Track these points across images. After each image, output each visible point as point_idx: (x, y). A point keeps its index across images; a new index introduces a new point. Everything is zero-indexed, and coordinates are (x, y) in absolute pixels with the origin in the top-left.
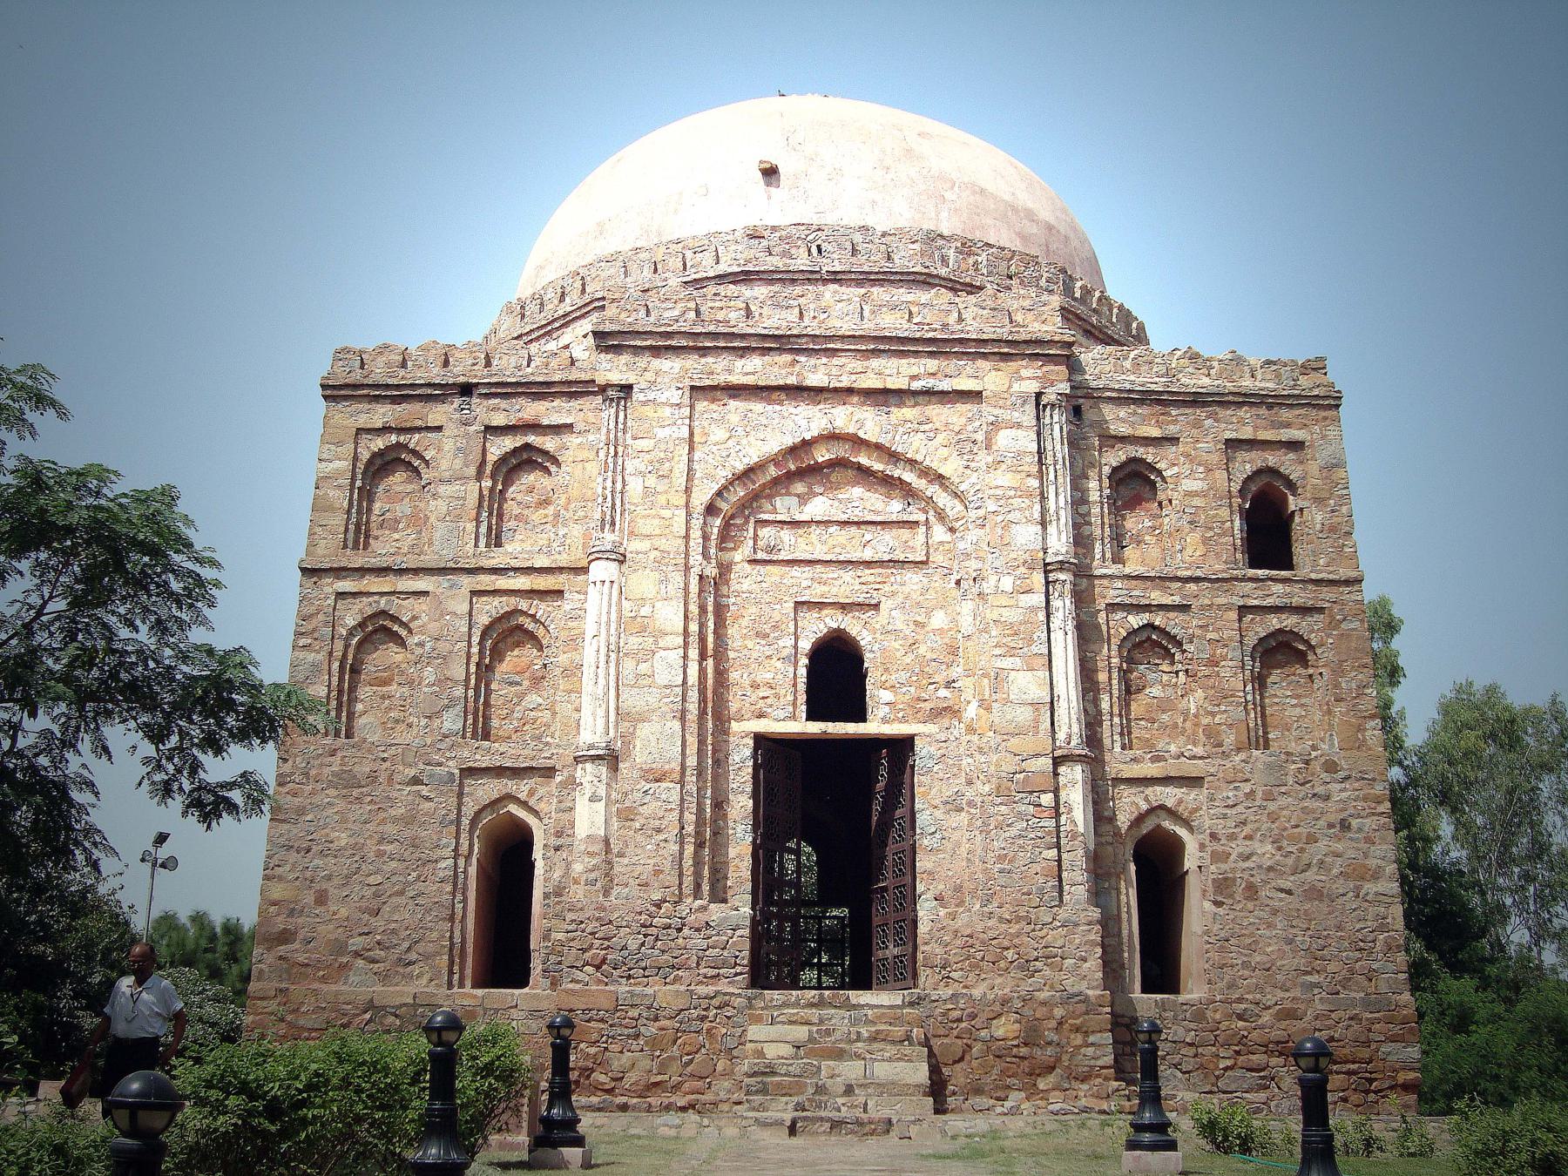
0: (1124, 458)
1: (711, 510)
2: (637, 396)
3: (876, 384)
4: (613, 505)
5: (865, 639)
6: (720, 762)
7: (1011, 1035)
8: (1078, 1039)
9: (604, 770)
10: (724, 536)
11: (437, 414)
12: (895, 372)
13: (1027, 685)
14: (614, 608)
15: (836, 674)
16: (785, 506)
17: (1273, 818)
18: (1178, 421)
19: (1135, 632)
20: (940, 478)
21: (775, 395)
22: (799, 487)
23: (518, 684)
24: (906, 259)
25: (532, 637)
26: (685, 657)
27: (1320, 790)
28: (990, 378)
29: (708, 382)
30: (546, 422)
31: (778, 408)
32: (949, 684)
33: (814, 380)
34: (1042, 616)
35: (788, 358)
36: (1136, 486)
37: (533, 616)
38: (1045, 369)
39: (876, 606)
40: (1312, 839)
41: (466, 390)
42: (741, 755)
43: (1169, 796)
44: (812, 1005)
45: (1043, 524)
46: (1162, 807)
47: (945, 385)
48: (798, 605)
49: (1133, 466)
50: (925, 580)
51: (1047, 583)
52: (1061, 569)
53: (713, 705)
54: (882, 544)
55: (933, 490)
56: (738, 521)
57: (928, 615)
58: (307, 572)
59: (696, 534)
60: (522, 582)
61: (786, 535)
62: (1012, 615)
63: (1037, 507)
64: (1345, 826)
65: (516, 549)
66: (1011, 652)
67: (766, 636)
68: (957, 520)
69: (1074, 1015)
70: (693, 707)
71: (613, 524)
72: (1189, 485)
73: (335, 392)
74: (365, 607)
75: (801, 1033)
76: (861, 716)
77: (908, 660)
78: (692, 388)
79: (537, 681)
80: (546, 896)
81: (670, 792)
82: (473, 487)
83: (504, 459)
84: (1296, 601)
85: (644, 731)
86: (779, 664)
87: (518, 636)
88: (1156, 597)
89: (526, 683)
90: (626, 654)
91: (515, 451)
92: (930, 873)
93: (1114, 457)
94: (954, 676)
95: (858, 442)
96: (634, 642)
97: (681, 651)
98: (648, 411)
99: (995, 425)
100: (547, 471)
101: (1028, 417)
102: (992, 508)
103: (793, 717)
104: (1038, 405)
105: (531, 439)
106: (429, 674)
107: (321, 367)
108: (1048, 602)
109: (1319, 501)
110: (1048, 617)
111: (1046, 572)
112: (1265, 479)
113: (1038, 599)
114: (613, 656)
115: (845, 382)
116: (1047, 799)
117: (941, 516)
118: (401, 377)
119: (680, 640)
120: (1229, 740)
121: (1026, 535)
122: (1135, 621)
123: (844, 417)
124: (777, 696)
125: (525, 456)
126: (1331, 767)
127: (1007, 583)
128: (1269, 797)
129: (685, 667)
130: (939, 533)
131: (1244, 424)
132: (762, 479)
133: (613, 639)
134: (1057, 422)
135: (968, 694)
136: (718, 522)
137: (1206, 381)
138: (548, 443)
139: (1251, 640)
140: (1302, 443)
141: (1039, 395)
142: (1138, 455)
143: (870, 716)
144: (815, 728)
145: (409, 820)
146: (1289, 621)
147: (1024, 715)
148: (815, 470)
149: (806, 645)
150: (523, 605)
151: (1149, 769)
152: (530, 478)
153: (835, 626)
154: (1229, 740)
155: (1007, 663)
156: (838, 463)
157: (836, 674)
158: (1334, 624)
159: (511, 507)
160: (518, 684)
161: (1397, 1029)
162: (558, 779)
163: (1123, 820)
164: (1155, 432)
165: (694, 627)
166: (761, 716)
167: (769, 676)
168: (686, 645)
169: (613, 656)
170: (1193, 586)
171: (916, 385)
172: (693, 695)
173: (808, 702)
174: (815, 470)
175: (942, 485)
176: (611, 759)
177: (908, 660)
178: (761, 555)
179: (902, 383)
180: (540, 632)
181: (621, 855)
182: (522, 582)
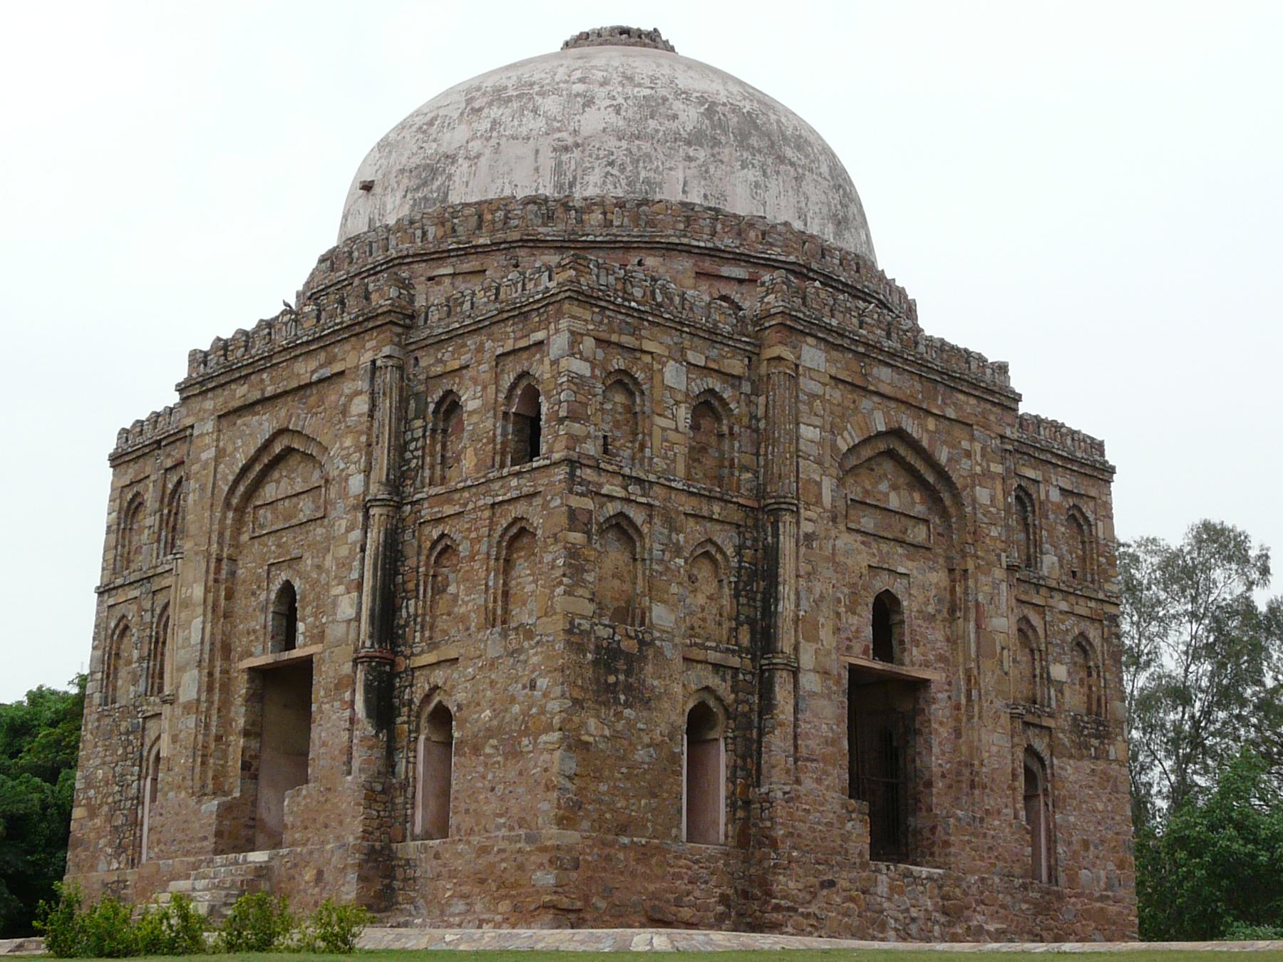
2: (196, 433)
16: (269, 491)
22: (276, 475)
26: (204, 622)
33: (270, 391)
42: (241, 687)
47: (327, 372)
54: (306, 508)
58: (100, 594)
67: (254, 594)
78: (219, 417)
81: (191, 721)
84: (525, 490)
88: (448, 510)
99: (351, 398)
107: (111, 445)
112: (524, 383)
122: (435, 535)
132: (252, 475)
140: (541, 343)
141: (374, 362)
146: (519, 510)
149: (273, 596)
156: (289, 451)
165: (210, 597)
168: (205, 615)
171: (315, 378)
172: (207, 647)
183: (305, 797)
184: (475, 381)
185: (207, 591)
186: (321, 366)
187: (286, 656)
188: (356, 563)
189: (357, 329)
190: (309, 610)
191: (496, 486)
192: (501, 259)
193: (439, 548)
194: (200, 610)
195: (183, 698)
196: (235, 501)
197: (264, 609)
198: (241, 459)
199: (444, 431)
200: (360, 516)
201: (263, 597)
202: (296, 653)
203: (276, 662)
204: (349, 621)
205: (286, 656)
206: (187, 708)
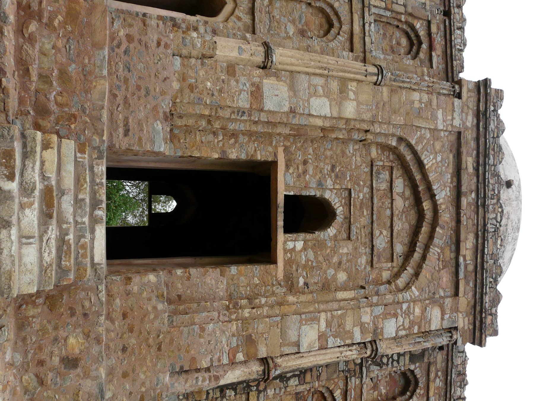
0: (418, 376)
2: (457, 101)
3: (462, 237)
4: (403, 82)
5: (331, 231)
7: (69, 348)
9: (260, 58)
10: (384, 147)
13: (309, 336)
14: (352, 76)
15: (309, 214)
16: (399, 185)
20: (417, 274)
21: (455, 179)
22: (408, 193)
23: (300, 22)
25: (327, 32)
26: (325, 117)
28: (465, 299)
29: (462, 141)
30: (433, 54)
31: (449, 181)
32: (306, 284)
33: (464, 201)
34: (348, 342)
35: (474, 187)
36: (401, 382)
37: (339, 34)
38: (468, 330)
39: (349, 238)
41: (447, 13)
44: (94, 193)
47: (461, 275)
48: (350, 191)
49: (413, 382)
50: (363, 267)
51: (364, 343)
52: (373, 350)
55: (410, 270)
56: (391, 157)
57: (344, 270)
59: (391, 130)
60: (357, 28)
61: (384, 186)
62: (349, 324)
63: (403, 333)
65: (372, 29)
66: (329, 324)
68: (396, 285)
71: (394, 80)
75: (69, 181)
76: (287, 230)
77: (321, 259)
78: (459, 133)
79: (302, 33)
80: (172, 19)
82: (402, 9)
85: (283, 90)
86: (317, 177)
87: (326, 26)
89: (300, 26)
90: (327, 80)
91: (418, 36)
92: (188, 278)
93: (418, 370)
94: (311, 288)
96: (334, 85)
97: (329, 115)
98: (450, 107)
100: (409, 53)
101: (446, 324)
102: (405, 306)
103: (287, 187)
104: (450, 328)
105: (424, 46)
108: (354, 344)
110: (349, 345)
111: (370, 342)
113: (358, 337)
114: (326, 72)
115: (464, 219)
117: (397, 275)
119: (335, 115)
121: (390, 328)
123: (446, 216)
124: (299, 176)
125: (415, 42)
127: (366, 318)
129: (320, 117)
130: (386, 275)
132: (414, 169)
133: (334, 73)
134: (443, 341)
135: (303, 298)
136: (394, 144)
138: (422, 55)
142: (420, 385)
143: (288, 235)
144: (281, 200)
147: (292, 336)
148: (418, 202)
149: (327, 195)
150: (346, 28)
152: (404, 41)
153: (338, 212)
157: (309, 214)
159: (391, 30)
160: (300, 22)
162: (248, 35)
166: (287, 167)
167: (311, 172)
168: (332, 118)
169: (326, 72)
171: (461, 259)
173: (294, 196)
174: (418, 202)
175: (412, 276)
177: (321, 259)
178: (375, 169)
179: (463, 251)
180: (329, 36)
181: (203, 64)
182: (357, 28)
183: (155, 308)
185: (348, 120)
186: (466, 266)
187: (280, 223)
188: (339, 342)
189: (478, 308)
190: (311, 254)
195: (269, 84)
196: (403, 149)
198: (428, 161)
200: (369, 339)
202: (281, 236)
203: (277, 207)
204: (298, 344)
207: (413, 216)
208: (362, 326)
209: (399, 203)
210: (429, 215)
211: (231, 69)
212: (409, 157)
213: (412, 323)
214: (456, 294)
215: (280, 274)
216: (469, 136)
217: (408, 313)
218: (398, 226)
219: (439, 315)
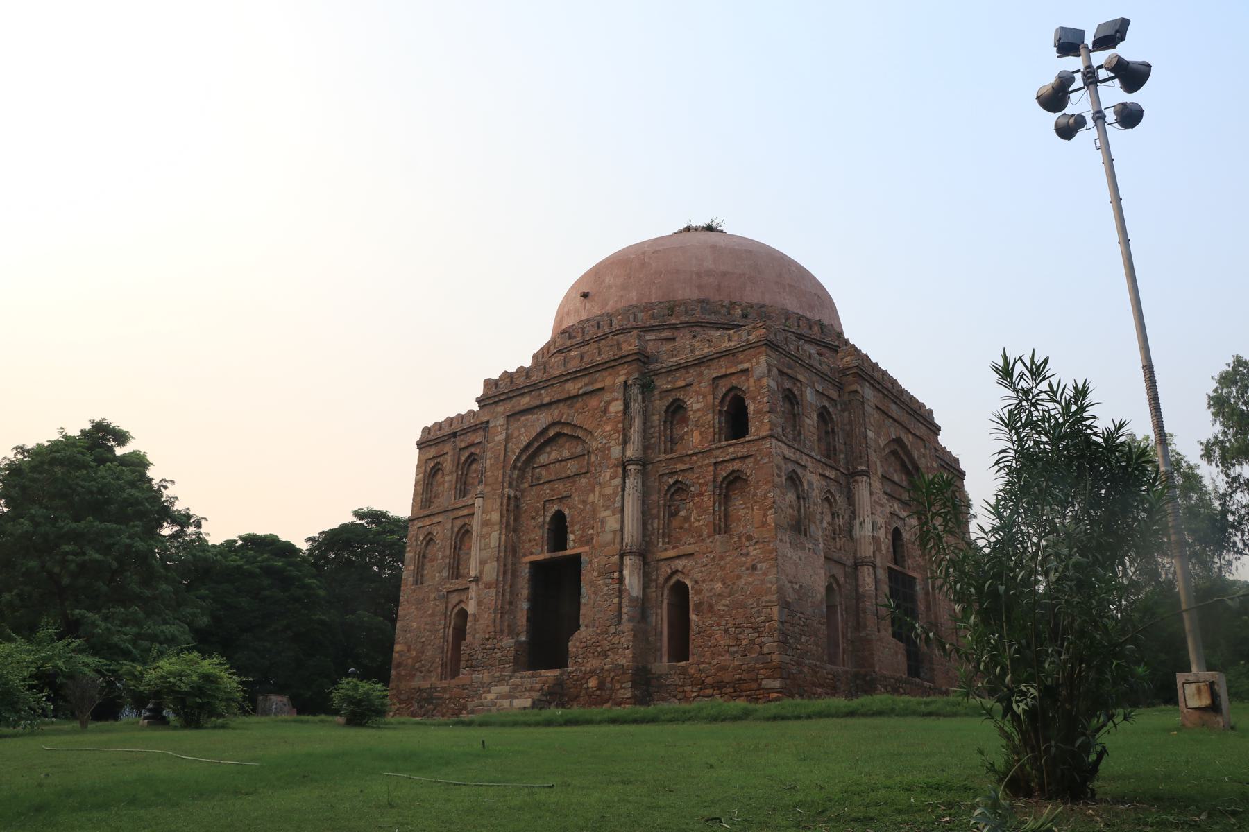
1: (514, 467)
2: (491, 425)
5: (567, 512)
6: (514, 574)
8: (618, 686)
11: (447, 448)
12: (572, 388)
16: (543, 459)
17: (722, 568)
18: (692, 375)
19: (670, 487)
22: (548, 449)
24: (591, 332)
27: (744, 551)
28: (606, 380)
33: (546, 400)
40: (739, 577)
41: (454, 435)
42: (525, 572)
43: (679, 564)
45: (625, 443)
46: (677, 571)
47: (590, 388)
53: (511, 550)
62: (609, 491)
64: (754, 568)
66: (607, 508)
67: (533, 518)
69: (617, 675)
70: (502, 554)
72: (695, 406)
73: (421, 445)
74: (424, 531)
81: (493, 591)
83: (466, 460)
84: (739, 455)
85: (487, 567)
88: (681, 467)
95: (559, 423)
99: (609, 403)
103: (542, 551)
106: (440, 555)
107: (418, 436)
109: (754, 399)
112: (731, 394)
113: (618, 481)
116: (616, 575)
118: (441, 433)
120: (705, 533)
121: (616, 451)
122: (671, 481)
126: (749, 538)
128: (721, 558)
131: (721, 368)
132: (531, 450)
137: (706, 350)
139: (720, 479)
140: (747, 370)
141: (626, 382)
145: (432, 615)
146: (737, 465)
149: (548, 519)
151: (672, 553)
152: (474, 466)
154: (705, 533)
155: (607, 513)
156: (559, 435)
157: (558, 529)
158: (756, 462)
161: (770, 672)
163: (661, 580)
164: (683, 384)
165: (504, 520)
166: (532, 553)
170: (694, 458)
172: (503, 548)
176: (476, 580)
179: (574, 392)
184: (698, 393)
185: (502, 516)
186: (586, 385)
187: (560, 554)
188: (619, 498)
190: (577, 527)
191: (718, 452)
192: (686, 331)
193: (673, 490)
194: (497, 527)
195: (485, 578)
197: (542, 526)
198: (525, 440)
199: (671, 423)
200: (620, 470)
201: (541, 520)
202: (568, 552)
203: (551, 558)
204: (614, 532)
205: (560, 554)
206: (488, 586)
207: (561, 441)
208: (611, 479)
209: (554, 455)
210: (557, 429)
211: (479, 603)
212: (524, 457)
213: (617, 431)
214: (602, 389)
215: (587, 549)
216: (507, 407)
217: (608, 437)
218: (566, 454)
219: (614, 404)
